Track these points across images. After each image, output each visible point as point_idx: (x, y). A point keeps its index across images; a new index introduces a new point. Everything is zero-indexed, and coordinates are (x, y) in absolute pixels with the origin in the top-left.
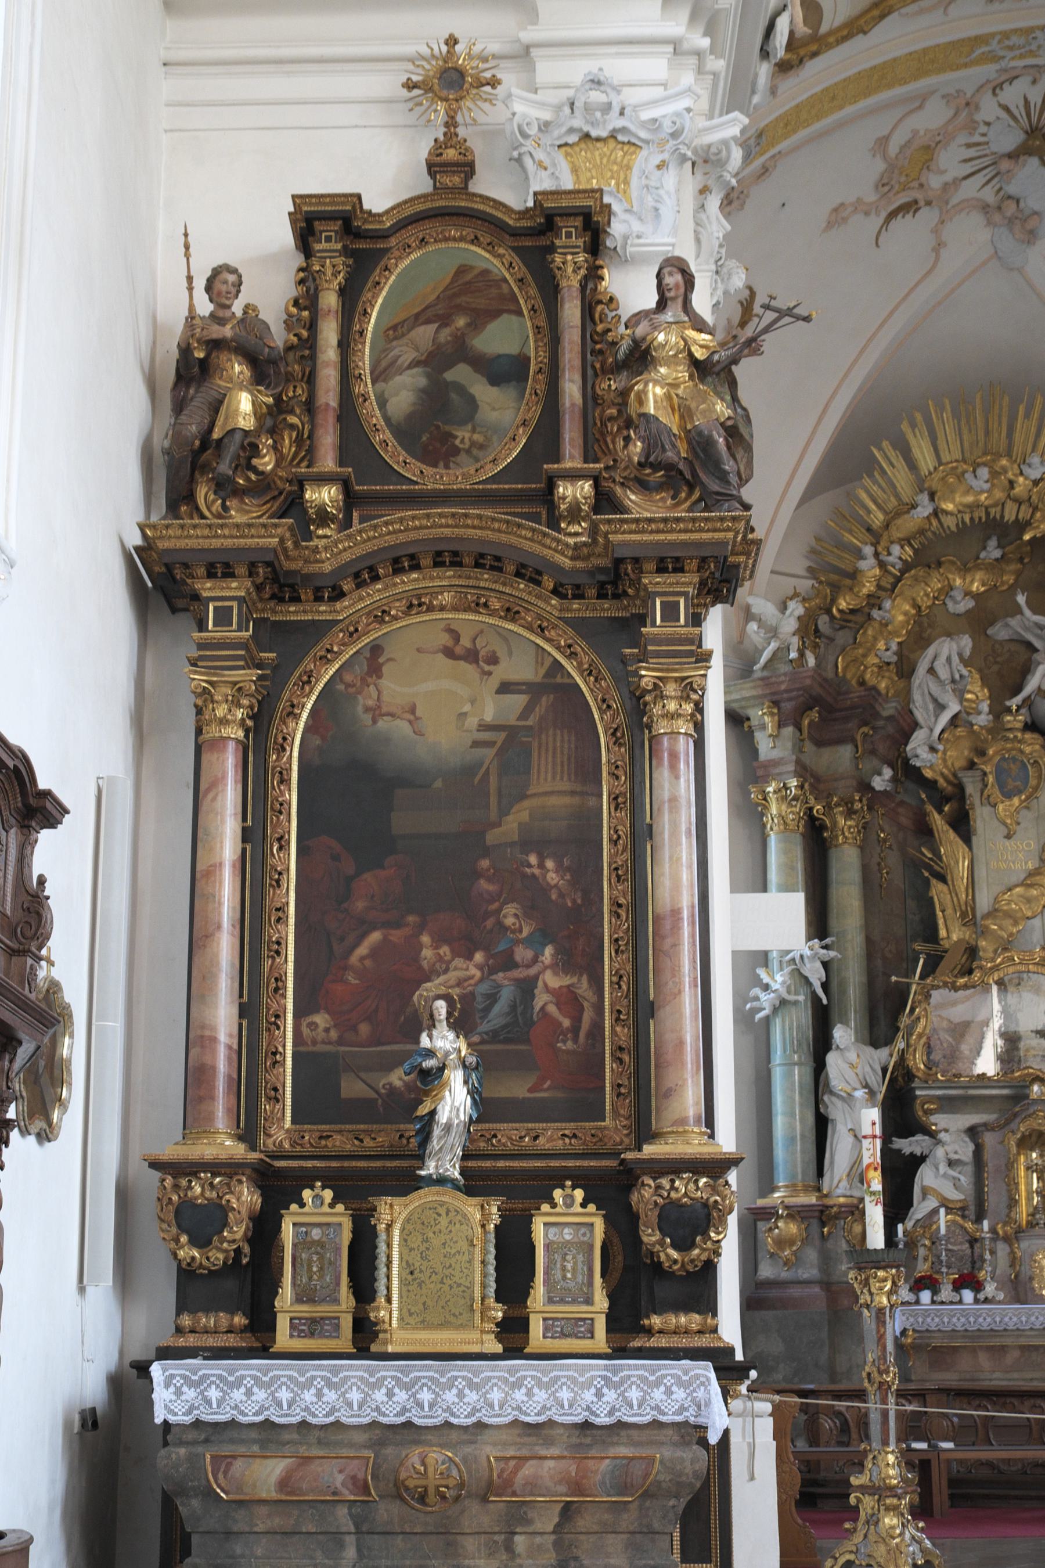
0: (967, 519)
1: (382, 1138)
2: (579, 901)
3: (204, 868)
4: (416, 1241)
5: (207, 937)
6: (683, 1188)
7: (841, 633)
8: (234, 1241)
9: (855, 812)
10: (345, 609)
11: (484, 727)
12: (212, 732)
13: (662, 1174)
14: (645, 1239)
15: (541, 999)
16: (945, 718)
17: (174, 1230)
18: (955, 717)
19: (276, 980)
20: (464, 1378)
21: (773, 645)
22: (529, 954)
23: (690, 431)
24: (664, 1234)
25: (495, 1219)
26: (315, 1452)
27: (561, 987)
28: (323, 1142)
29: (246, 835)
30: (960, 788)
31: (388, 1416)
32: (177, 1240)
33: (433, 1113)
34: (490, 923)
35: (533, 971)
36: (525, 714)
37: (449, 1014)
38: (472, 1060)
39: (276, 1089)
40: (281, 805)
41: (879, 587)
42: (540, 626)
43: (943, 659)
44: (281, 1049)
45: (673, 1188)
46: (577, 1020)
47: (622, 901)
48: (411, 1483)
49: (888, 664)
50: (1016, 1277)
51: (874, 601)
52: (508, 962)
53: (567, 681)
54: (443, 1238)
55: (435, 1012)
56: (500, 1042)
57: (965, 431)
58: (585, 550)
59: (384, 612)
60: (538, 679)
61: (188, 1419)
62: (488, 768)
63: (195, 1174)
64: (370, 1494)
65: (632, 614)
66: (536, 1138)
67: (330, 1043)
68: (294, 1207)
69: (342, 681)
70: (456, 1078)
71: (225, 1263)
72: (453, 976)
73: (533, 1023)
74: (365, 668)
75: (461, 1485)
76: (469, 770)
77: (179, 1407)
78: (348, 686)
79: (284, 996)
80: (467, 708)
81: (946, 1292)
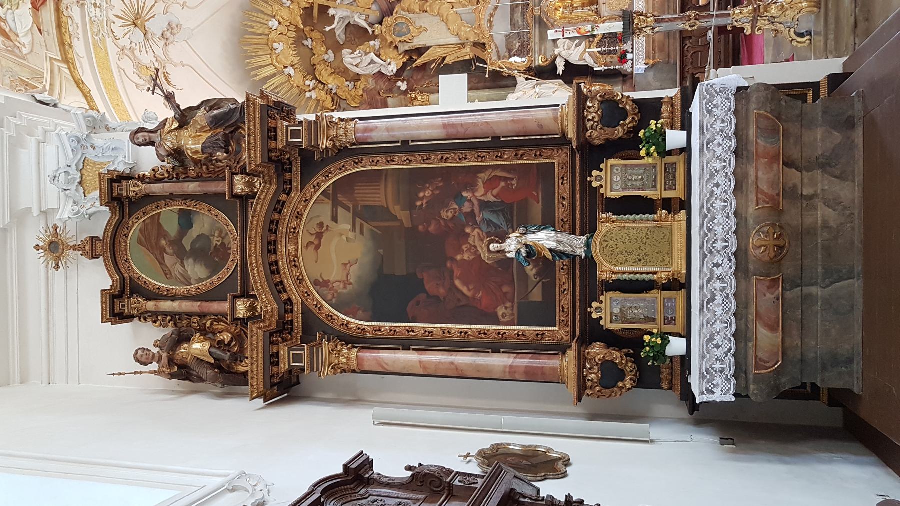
1: (562, 278)
2: (440, 179)
3: (422, 370)
4: (622, 258)
5: (457, 369)
6: (593, 112)
7: (342, 106)
8: (621, 357)
9: (416, 96)
10: (296, 297)
11: (354, 229)
12: (354, 365)
13: (585, 126)
14: (621, 135)
15: (490, 198)
16: (376, 59)
17: (616, 389)
18: (376, 55)
19: (480, 334)
20: (708, 223)
22: (467, 204)
23: (211, 128)
24: (619, 125)
25: (610, 215)
26: (753, 310)
27: (484, 187)
28: (566, 310)
29: (406, 348)
30: (406, 52)
31: (731, 266)
32: (622, 387)
33: (551, 250)
34: (451, 225)
35: (476, 202)
36: (348, 209)
37: (497, 242)
38: (522, 230)
39: (538, 335)
40: (391, 330)
41: (323, 90)
42: (305, 202)
44: (516, 332)
45: (592, 120)
46: (501, 178)
47: (440, 157)
48: (772, 254)
49: (355, 85)
52: (472, 214)
53: (331, 186)
54: (620, 244)
55: (496, 249)
56: (512, 218)
57: (259, 54)
58: (266, 178)
59: (298, 279)
60: (331, 202)
61: (733, 381)
62: (374, 227)
63: (585, 377)
64: (778, 278)
65: (299, 156)
66: (564, 198)
67: (513, 306)
68: (602, 322)
69: (331, 300)
70: (532, 238)
71: (633, 362)
72: (477, 243)
73: (502, 201)
74: (325, 288)
75: (773, 225)
76: (374, 236)
77: (726, 386)
78: (334, 297)
79: (489, 330)
80: (344, 238)
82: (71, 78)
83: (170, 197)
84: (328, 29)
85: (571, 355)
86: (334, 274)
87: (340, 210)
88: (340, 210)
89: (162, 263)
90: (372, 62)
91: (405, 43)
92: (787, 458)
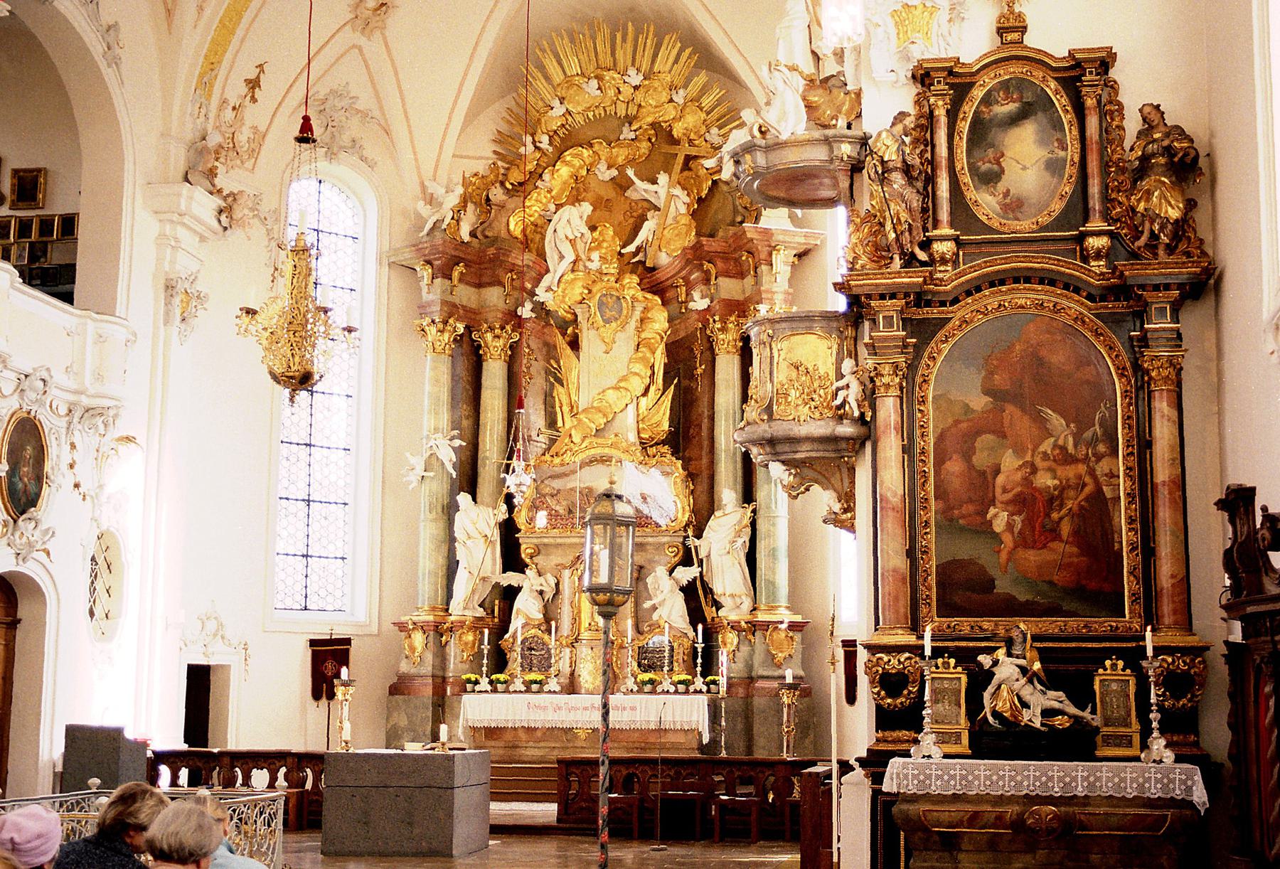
0: (591, 115)
9: (498, 337)
21: (434, 219)
43: (564, 220)
51: (537, 175)
90: (562, 257)
91: (588, 315)
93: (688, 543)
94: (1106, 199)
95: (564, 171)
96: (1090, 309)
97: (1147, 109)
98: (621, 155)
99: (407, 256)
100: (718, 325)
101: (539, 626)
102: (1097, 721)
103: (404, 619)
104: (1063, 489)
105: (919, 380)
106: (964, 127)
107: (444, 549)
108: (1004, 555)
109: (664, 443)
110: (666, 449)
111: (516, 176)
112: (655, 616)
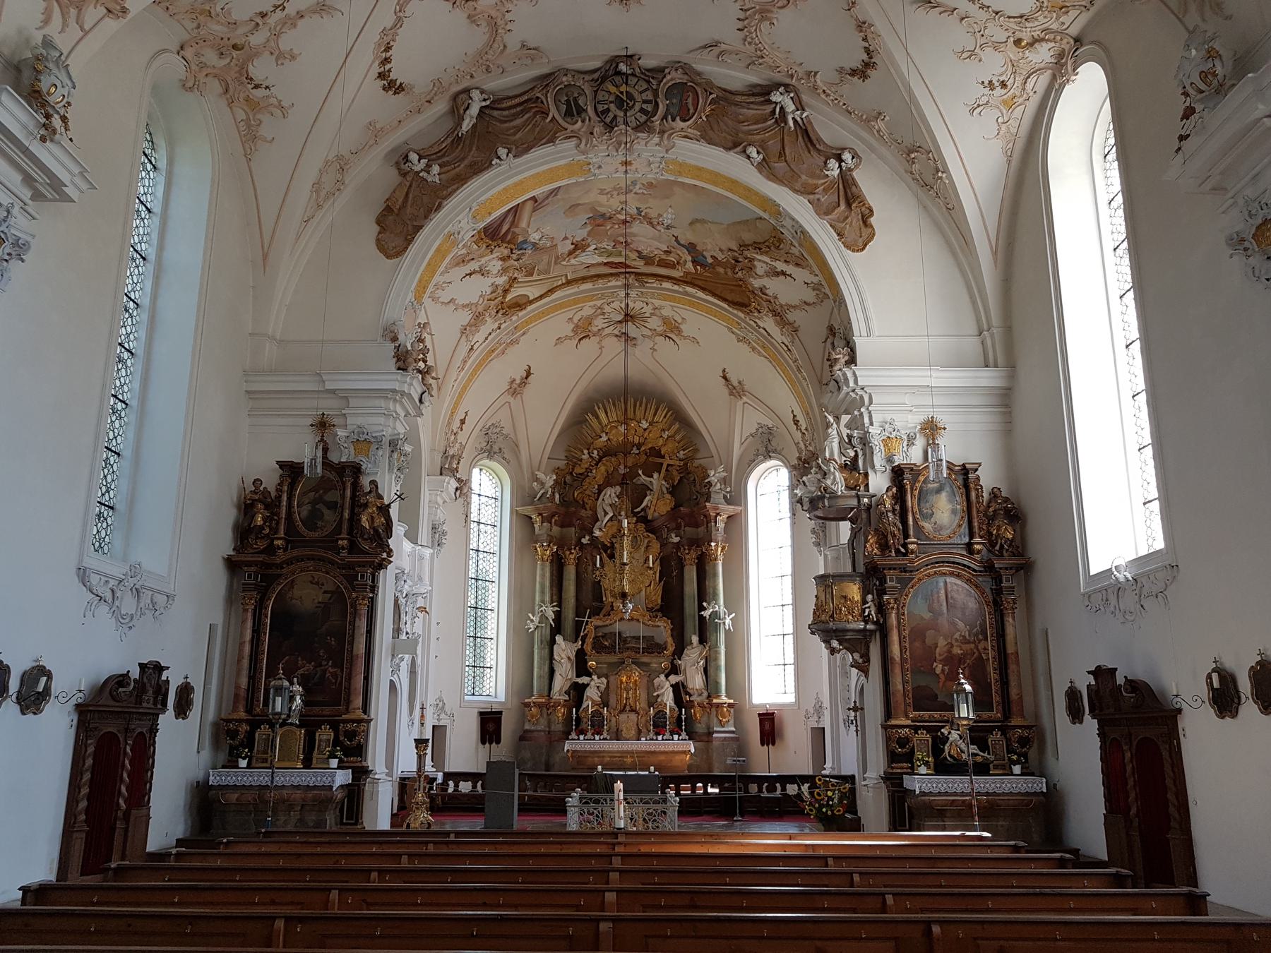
10: (284, 571)
11: (319, 603)
21: (542, 492)
30: (612, 544)
36: (330, 599)
43: (608, 496)
50: (617, 730)
51: (589, 470)
77: (215, 781)
81: (589, 735)
82: (555, 285)
83: (343, 497)
84: (640, 472)
85: (242, 715)
86: (297, 592)
87: (330, 595)
88: (330, 595)
89: (310, 491)
92: (188, 807)
93: (675, 662)
94: (980, 528)
95: (603, 468)
96: (973, 575)
97: (995, 490)
98: (630, 461)
99: (527, 510)
100: (687, 552)
101: (599, 705)
102: (992, 757)
103: (526, 701)
104: (965, 655)
105: (901, 605)
106: (916, 493)
107: (547, 662)
108: (941, 684)
109: (658, 610)
110: (660, 614)
111: (578, 470)
112: (659, 700)
